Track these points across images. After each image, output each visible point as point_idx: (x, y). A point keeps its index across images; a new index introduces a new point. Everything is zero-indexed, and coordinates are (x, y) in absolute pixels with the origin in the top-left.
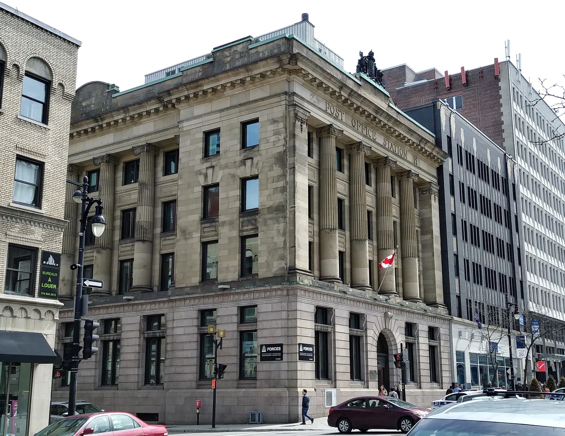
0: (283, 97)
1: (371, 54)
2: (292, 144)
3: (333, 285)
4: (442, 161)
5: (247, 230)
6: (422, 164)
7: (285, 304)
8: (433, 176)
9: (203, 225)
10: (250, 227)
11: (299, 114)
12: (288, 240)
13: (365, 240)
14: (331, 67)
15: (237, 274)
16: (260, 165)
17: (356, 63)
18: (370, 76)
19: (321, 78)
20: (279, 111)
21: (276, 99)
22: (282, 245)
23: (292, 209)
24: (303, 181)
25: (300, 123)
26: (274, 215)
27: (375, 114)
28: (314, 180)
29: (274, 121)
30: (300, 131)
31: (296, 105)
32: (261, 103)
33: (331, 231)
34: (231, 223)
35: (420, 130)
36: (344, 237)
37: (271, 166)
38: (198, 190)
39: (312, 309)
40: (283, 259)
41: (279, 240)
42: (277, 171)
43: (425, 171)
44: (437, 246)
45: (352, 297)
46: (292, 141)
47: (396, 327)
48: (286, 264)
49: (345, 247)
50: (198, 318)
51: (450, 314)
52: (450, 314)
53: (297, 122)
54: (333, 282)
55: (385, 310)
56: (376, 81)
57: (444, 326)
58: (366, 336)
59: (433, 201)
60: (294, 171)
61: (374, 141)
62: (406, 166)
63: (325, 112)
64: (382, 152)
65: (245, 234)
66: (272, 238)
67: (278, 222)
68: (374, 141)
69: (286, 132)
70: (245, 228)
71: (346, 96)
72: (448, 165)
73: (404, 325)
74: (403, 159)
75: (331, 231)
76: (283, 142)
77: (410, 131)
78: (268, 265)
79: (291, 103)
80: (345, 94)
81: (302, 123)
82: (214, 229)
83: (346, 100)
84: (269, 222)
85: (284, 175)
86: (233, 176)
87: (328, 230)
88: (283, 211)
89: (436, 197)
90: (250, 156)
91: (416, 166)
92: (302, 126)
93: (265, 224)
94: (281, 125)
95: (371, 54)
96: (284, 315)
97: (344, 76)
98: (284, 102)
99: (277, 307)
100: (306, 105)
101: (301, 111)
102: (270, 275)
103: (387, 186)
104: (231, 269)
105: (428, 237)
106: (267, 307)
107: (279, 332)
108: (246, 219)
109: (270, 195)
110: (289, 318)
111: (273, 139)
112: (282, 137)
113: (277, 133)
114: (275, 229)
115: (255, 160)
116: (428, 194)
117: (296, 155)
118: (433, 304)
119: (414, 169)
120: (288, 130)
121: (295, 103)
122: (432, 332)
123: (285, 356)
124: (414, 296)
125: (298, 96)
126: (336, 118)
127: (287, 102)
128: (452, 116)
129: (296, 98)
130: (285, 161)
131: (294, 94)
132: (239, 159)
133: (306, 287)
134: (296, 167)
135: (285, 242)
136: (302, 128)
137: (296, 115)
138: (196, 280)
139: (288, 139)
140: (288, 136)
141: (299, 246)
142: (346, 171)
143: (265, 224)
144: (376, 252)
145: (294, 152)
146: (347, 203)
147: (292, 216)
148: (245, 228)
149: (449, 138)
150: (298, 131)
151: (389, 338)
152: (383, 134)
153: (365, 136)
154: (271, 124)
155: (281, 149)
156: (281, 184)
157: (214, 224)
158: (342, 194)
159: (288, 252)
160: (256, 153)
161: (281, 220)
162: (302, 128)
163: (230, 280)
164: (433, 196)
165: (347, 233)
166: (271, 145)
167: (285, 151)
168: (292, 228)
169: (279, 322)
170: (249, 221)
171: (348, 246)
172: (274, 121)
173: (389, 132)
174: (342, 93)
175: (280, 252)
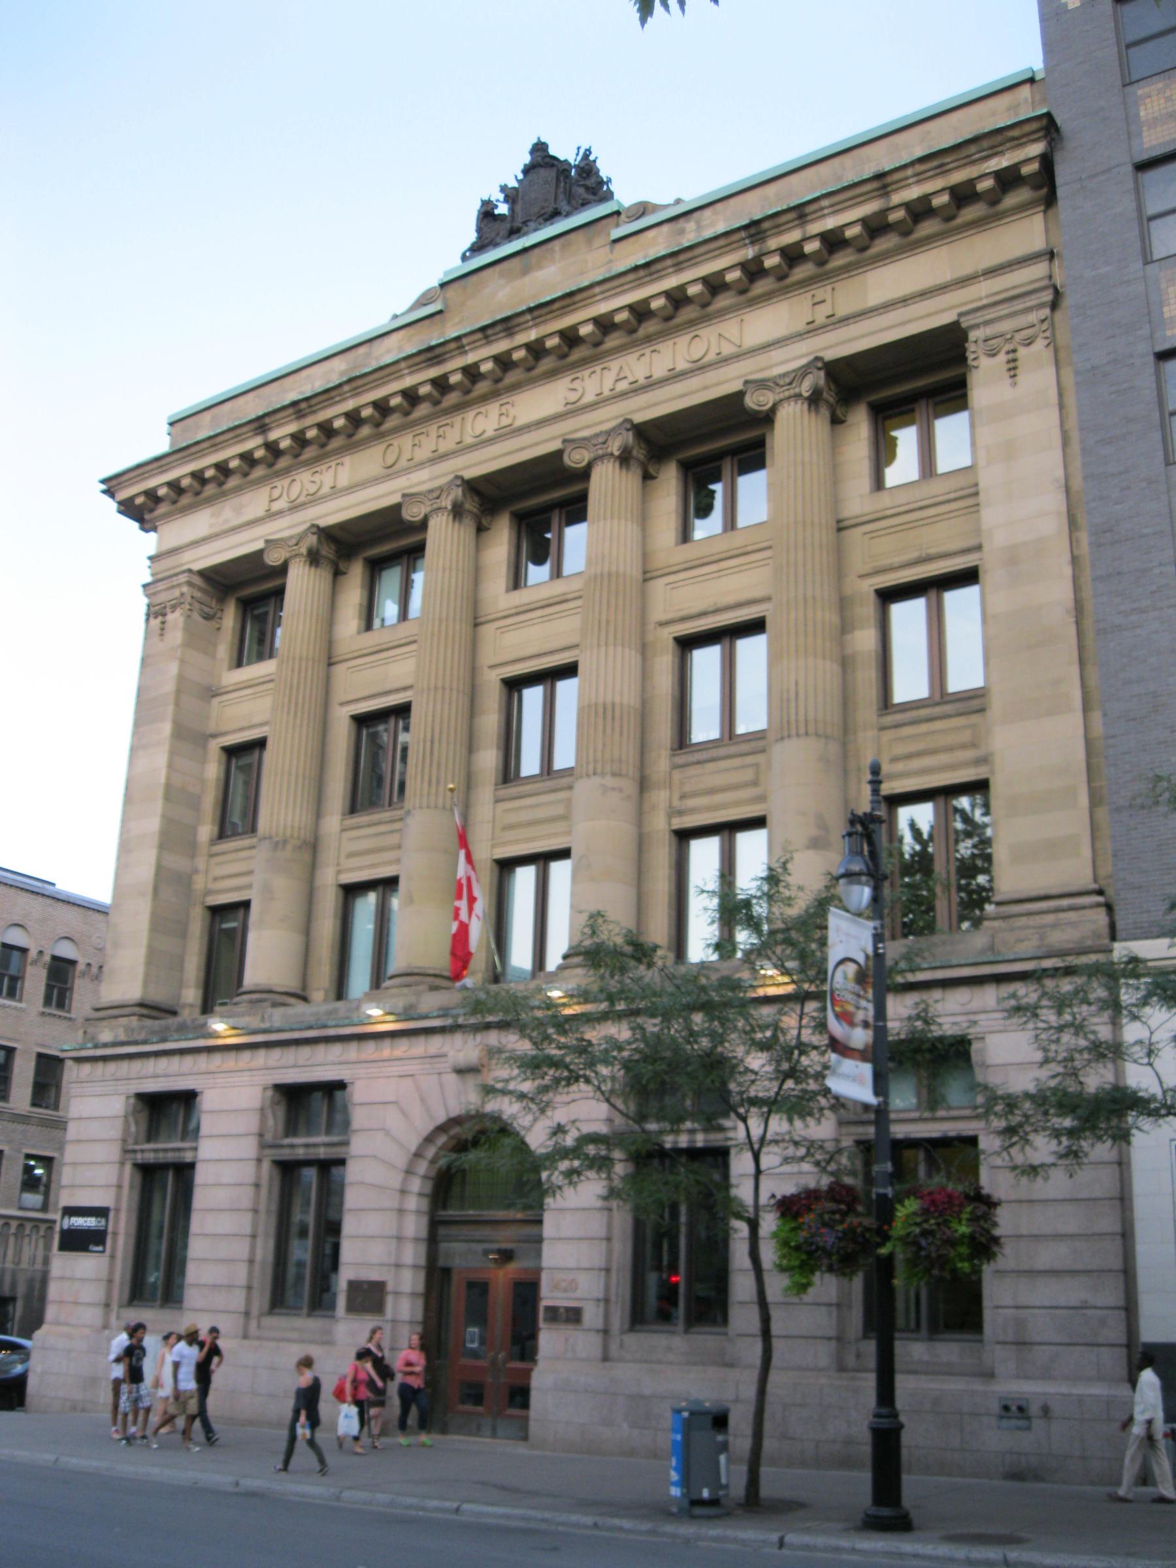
14: (304, 373)
80: (281, 433)
83: (300, 440)
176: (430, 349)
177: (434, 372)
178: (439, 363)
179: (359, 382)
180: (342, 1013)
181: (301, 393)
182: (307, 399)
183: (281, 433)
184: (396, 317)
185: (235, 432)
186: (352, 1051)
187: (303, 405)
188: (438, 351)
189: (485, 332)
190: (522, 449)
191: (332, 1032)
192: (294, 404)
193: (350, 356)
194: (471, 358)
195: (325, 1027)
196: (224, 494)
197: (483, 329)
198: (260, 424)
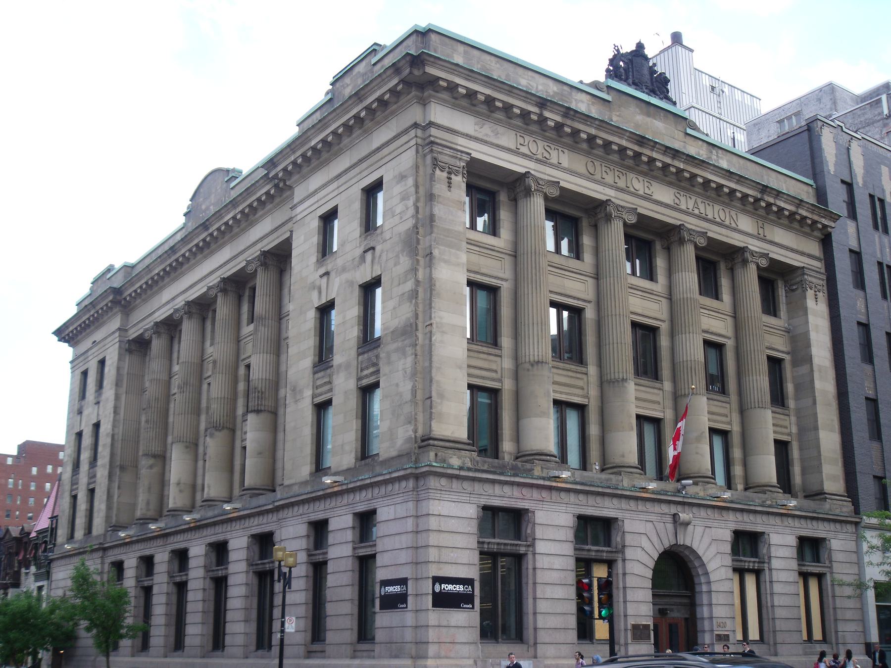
0: (412, 133)
1: (640, 46)
2: (428, 213)
3: (528, 466)
4: (825, 226)
5: (367, 376)
6: (781, 235)
7: (411, 505)
8: (810, 256)
9: (317, 376)
10: (371, 370)
11: (441, 157)
12: (419, 386)
13: (624, 380)
14: (530, 73)
15: (353, 455)
16: (384, 257)
17: (605, 64)
18: (636, 85)
19: (488, 92)
20: (407, 159)
21: (404, 139)
22: (408, 396)
23: (428, 328)
24: (452, 275)
25: (445, 174)
26: (399, 344)
27: (636, 148)
28: (501, 275)
29: (402, 177)
30: (445, 187)
31: (432, 143)
32: (386, 151)
33: (532, 365)
34: (348, 366)
35: (773, 174)
36: (584, 377)
37: (397, 256)
38: (311, 315)
39: (471, 511)
40: (410, 423)
41: (406, 387)
42: (405, 262)
43: (789, 247)
44: (825, 385)
45: (578, 487)
46: (428, 209)
47: (706, 540)
48: (415, 431)
49: (587, 397)
50: (308, 536)
51: (857, 511)
52: (857, 511)
53: (438, 172)
54: (531, 462)
55: (673, 509)
56: (652, 92)
57: (841, 536)
58: (624, 560)
59: (810, 303)
60: (431, 260)
61: (647, 198)
62: (736, 240)
63: (516, 152)
64: (670, 217)
65: (365, 382)
66: (397, 385)
67: (404, 354)
68: (647, 198)
69: (417, 192)
70: (366, 372)
71: (558, 119)
72: (846, 235)
73: (728, 536)
74: (727, 227)
75: (532, 365)
76: (411, 211)
77: (729, 174)
78: (392, 432)
79: (427, 141)
80: (553, 117)
81: (449, 173)
82: (326, 380)
83: (559, 127)
84: (394, 357)
85: (414, 270)
86: (351, 283)
87: (527, 366)
88: (416, 332)
89: (820, 295)
90: (372, 245)
91: (764, 239)
92: (450, 178)
93: (389, 363)
94: (410, 181)
95: (640, 46)
96: (410, 524)
97: (566, 88)
98: (413, 142)
99: (401, 510)
100: (461, 141)
101: (447, 151)
102: (394, 453)
103: (689, 279)
104: (347, 448)
105: (804, 369)
106: (391, 512)
107: (404, 557)
108: (366, 355)
109: (394, 308)
110: (420, 529)
111: (398, 210)
112: (411, 203)
113: (404, 198)
114: (400, 368)
115: (378, 248)
116: (799, 291)
117: (435, 230)
118: (818, 495)
119: (755, 245)
120: (422, 191)
121: (432, 139)
122: (811, 548)
123: (410, 600)
124: (764, 480)
125: (439, 127)
126: (544, 162)
127: (419, 141)
128: (854, 145)
129: (433, 131)
130: (419, 244)
131: (431, 124)
132: (359, 251)
133: (450, 471)
134: (436, 252)
135: (414, 392)
136: (450, 183)
137: (435, 163)
138: (306, 470)
139: (420, 205)
140: (422, 199)
141: (441, 396)
142: (588, 257)
143: (389, 363)
144: (669, 403)
145: (432, 226)
146: (590, 314)
147: (427, 342)
148: (366, 372)
149: (849, 186)
150: (440, 188)
151: (691, 561)
152: (670, 184)
153: (621, 190)
154: (398, 183)
155: (410, 223)
156: (409, 285)
157: (328, 371)
158: (579, 299)
159: (420, 408)
160: (379, 238)
161: (409, 350)
162: (450, 183)
163: (345, 467)
164: (810, 293)
165: (592, 370)
166: (397, 219)
167: (416, 227)
168: (427, 364)
169: (404, 537)
170: (369, 359)
171: (594, 392)
172: (402, 177)
173: (683, 181)
174: (547, 114)
175: (408, 409)
176: (644, 138)
177: (636, 148)
178: (641, 146)
179: (604, 125)
180: (614, 482)
181: (508, 75)
182: (576, 112)
183: (553, 117)
184: (581, 82)
185: (527, 95)
186: (624, 504)
187: (572, 113)
188: (645, 141)
189: (667, 150)
190: (664, 215)
191: (619, 492)
192: (569, 109)
193: (560, 86)
194: (655, 155)
195: (617, 489)
196: (489, 117)
197: (667, 147)
198: (543, 103)
